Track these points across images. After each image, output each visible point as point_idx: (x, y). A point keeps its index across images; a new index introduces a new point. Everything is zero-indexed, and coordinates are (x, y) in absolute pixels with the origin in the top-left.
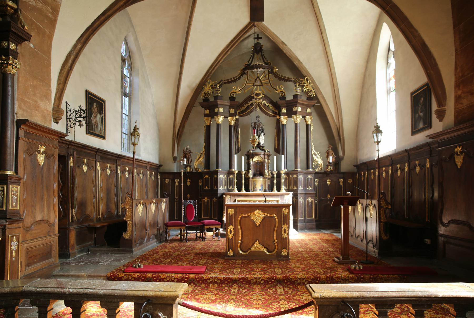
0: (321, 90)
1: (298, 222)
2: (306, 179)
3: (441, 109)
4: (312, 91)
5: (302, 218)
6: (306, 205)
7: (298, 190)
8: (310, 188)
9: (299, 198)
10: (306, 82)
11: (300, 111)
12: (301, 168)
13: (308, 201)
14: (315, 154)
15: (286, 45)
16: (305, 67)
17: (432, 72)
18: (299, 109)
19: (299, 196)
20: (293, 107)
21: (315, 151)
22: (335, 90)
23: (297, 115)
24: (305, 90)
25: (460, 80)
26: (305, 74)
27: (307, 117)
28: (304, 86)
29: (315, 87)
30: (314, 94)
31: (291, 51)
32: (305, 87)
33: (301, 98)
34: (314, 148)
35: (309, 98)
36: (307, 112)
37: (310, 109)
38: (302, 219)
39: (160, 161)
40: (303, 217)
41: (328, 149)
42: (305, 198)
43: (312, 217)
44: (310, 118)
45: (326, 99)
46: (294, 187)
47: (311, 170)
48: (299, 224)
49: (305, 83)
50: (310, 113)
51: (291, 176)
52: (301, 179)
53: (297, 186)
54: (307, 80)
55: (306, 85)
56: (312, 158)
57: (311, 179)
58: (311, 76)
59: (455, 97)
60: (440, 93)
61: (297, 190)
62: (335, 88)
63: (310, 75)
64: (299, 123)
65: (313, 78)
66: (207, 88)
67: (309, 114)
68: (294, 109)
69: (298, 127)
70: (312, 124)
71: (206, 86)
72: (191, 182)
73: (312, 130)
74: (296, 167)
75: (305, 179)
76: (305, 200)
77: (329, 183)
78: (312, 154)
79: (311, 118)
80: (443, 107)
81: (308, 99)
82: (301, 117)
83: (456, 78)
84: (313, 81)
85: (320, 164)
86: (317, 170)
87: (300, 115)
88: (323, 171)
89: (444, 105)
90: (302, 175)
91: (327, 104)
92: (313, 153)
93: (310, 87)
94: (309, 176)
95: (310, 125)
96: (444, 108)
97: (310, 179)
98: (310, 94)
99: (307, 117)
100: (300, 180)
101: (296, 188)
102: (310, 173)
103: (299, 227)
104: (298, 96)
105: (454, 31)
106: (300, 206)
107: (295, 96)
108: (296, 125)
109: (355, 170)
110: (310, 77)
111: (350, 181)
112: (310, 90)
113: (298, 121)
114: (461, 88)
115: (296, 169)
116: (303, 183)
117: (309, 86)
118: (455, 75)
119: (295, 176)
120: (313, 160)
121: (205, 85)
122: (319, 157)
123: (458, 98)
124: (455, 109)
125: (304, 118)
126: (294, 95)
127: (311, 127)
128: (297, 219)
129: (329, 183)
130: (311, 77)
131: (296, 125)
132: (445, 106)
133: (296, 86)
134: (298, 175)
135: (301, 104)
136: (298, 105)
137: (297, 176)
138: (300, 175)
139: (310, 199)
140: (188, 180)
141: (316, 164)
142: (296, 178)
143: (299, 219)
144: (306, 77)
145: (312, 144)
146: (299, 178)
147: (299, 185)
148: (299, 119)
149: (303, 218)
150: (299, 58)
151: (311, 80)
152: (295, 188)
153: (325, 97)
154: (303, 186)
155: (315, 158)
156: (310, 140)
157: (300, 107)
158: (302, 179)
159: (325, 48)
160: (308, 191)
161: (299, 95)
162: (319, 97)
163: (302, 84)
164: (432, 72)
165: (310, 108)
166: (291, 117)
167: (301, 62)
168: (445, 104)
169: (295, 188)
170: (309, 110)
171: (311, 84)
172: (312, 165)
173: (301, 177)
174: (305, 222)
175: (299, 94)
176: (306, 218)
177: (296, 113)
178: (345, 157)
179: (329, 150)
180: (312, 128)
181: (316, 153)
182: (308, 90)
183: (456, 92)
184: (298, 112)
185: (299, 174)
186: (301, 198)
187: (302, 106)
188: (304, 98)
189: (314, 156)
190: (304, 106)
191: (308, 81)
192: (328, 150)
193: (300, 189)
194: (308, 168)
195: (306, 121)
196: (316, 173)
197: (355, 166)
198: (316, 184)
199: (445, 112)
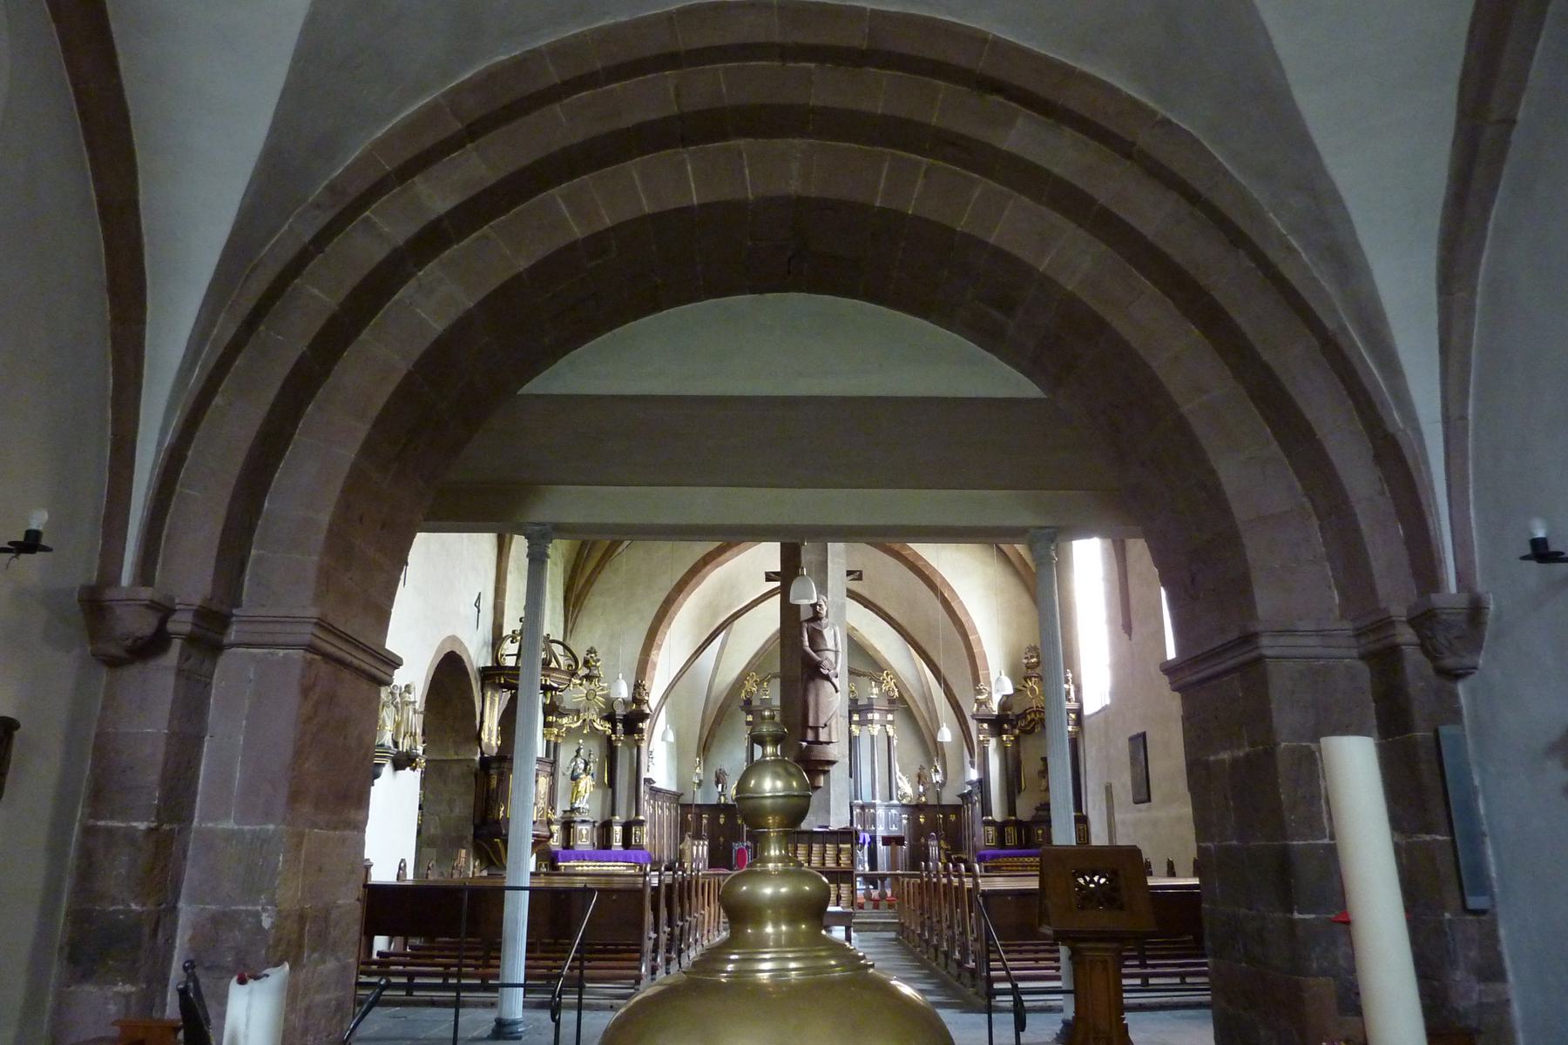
12: (880, 799)
14: (900, 779)
15: (857, 630)
26: (884, 666)
27: (888, 726)
30: (897, 694)
31: (864, 637)
35: (892, 701)
39: (678, 788)
49: (884, 679)
51: (867, 810)
56: (897, 783)
63: (892, 668)
66: (751, 686)
67: (891, 723)
68: (870, 716)
71: (748, 681)
72: (725, 818)
73: (895, 744)
74: (874, 797)
75: (887, 815)
77: (922, 820)
84: (896, 676)
86: (904, 802)
88: (914, 803)
94: (893, 811)
99: (888, 726)
102: (894, 806)
108: (872, 737)
109: (959, 801)
111: (953, 818)
113: (875, 733)
120: (898, 788)
121: (746, 679)
122: (906, 782)
129: (922, 820)
131: (872, 737)
140: (722, 816)
146: (877, 813)
147: (878, 824)
150: (876, 646)
151: (894, 675)
152: (873, 828)
155: (900, 784)
162: (906, 696)
167: (878, 651)
170: (890, 717)
172: (897, 794)
173: (881, 812)
177: (871, 722)
180: (895, 742)
181: (902, 777)
189: (898, 780)
194: (891, 798)
195: (887, 732)
196: (903, 805)
197: (959, 796)
198: (905, 822)
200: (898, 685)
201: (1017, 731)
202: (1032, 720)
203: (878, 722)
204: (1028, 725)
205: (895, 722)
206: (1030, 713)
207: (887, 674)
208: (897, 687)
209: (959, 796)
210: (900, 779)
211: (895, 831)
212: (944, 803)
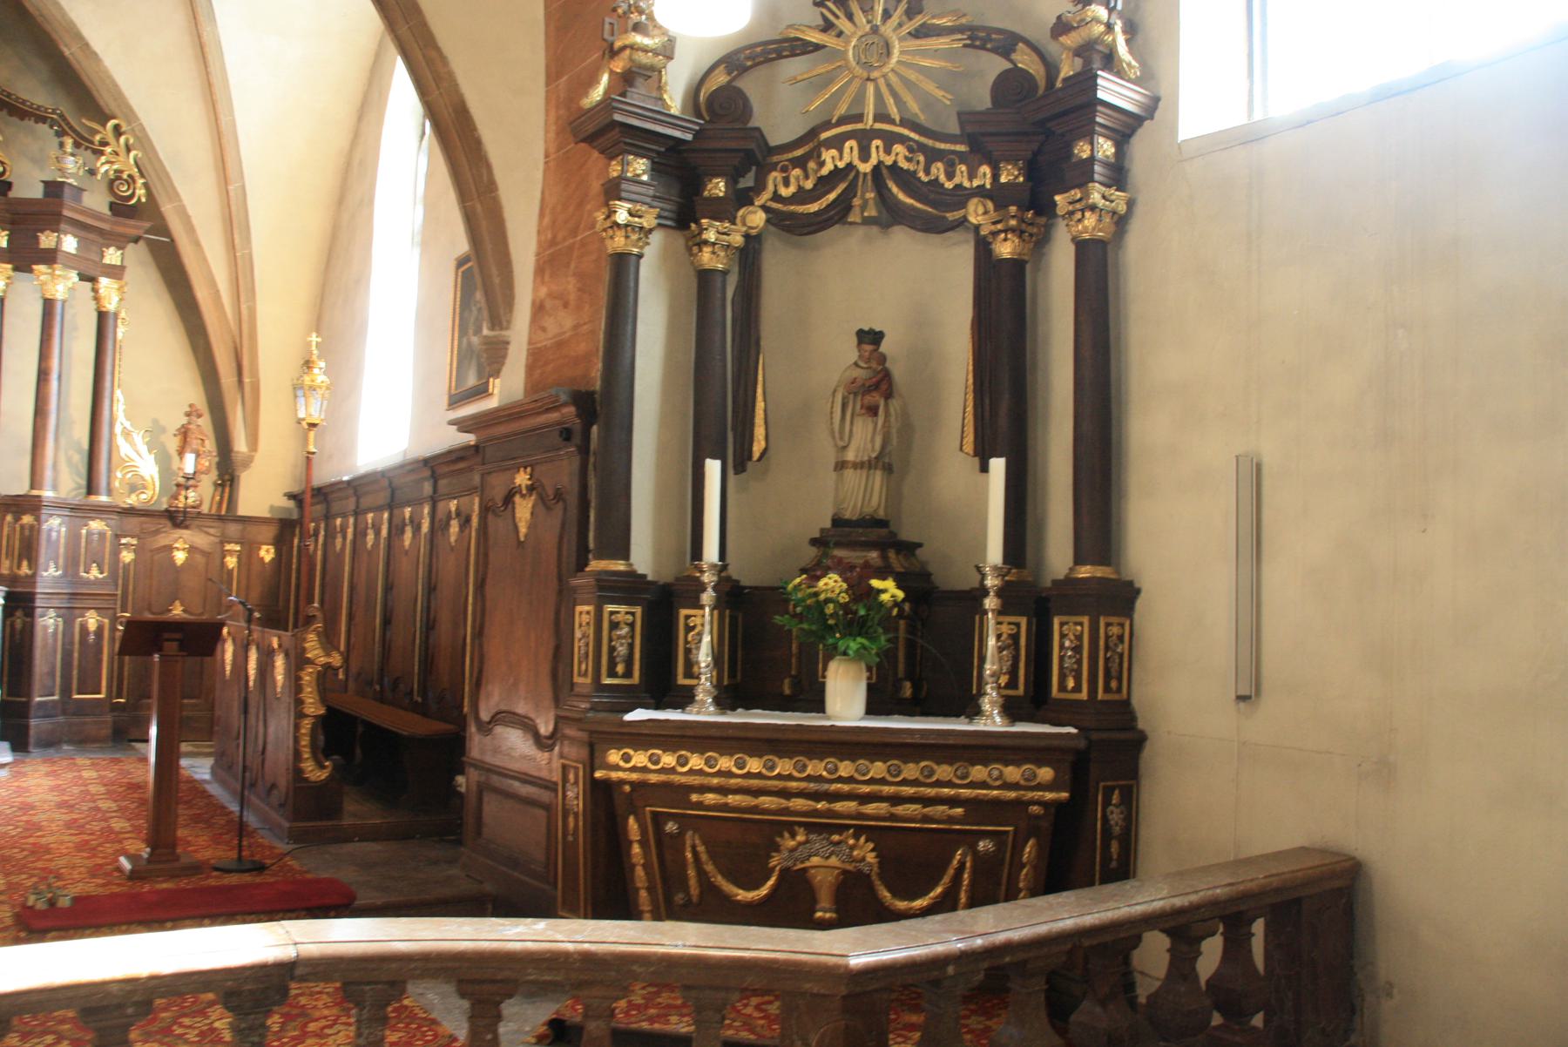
0: (176, 184)
1: (32, 712)
2: (79, 536)
3: (495, 337)
4: (134, 182)
5: (53, 695)
6: (72, 643)
7: (38, 579)
8: (95, 573)
9: (38, 611)
10: (110, 137)
11: (74, 252)
13: (84, 629)
14: (127, 434)
16: (110, 77)
17: (479, 207)
18: (70, 244)
19: (38, 603)
20: (42, 231)
21: (128, 424)
22: (232, 194)
23: (56, 266)
24: (103, 170)
25: (547, 253)
28: (102, 153)
29: (149, 166)
30: (141, 192)
32: (103, 159)
33: (78, 199)
34: (124, 411)
35: (121, 208)
36: (107, 261)
37: (119, 252)
38: (53, 701)
40: (57, 690)
41: (184, 420)
42: (69, 614)
43: (99, 693)
44: (116, 286)
45: (195, 221)
46: (19, 567)
47: (103, 499)
48: (33, 722)
49: (104, 143)
50: (114, 266)
52: (54, 534)
53: (33, 562)
54: (118, 131)
55: (108, 150)
57: (102, 535)
58: (137, 119)
59: (534, 303)
60: (497, 280)
61: (34, 576)
62: (231, 188)
63: (131, 116)
64: (64, 302)
65: (143, 129)
67: (116, 272)
68: (47, 240)
69: (58, 318)
70: (123, 314)
75: (74, 538)
76: (69, 623)
78: (112, 433)
79: (120, 289)
80: (501, 329)
81: (112, 206)
82: (76, 279)
83: (539, 243)
84: (144, 141)
85: (148, 478)
86: (132, 500)
87: (68, 267)
89: (505, 324)
90: (59, 515)
91: (197, 244)
92: (118, 429)
93: (127, 164)
94: (96, 525)
95: (116, 315)
96: (504, 333)
97: (96, 537)
98: (123, 190)
99: (104, 282)
100: (49, 536)
101: (30, 568)
103: (32, 732)
104: (67, 191)
105: (547, 92)
106: (45, 646)
107: (54, 189)
110: (129, 123)
112: (125, 176)
113: (59, 291)
114: (547, 278)
115: (35, 492)
116: (62, 550)
117: (121, 159)
118: (539, 232)
119: (27, 519)
122: (143, 449)
123: (539, 309)
124: (530, 342)
125: (88, 285)
126: (46, 184)
127: (116, 326)
128: (24, 699)
130: (134, 125)
131: (48, 306)
132: (507, 328)
133: (62, 145)
134: (43, 517)
135: (80, 227)
136: (63, 226)
137: (38, 519)
138: (51, 515)
139: (92, 621)
141: (129, 475)
142: (32, 527)
143: (38, 699)
144: (114, 117)
145: (118, 393)
146: (45, 527)
147: (42, 559)
148: (62, 284)
149: (56, 698)
151: (136, 137)
153: (191, 211)
154: (61, 561)
155: (123, 448)
156: (108, 378)
157: (75, 236)
158: (59, 532)
159: (196, 24)
160: (88, 583)
161: (70, 184)
162: (167, 208)
163: (92, 143)
164: (479, 207)
165: (119, 248)
166: (31, 271)
168: (509, 322)
169: (25, 570)
171: (132, 154)
173: (54, 526)
174: (64, 713)
175: (70, 181)
176: (70, 697)
177: (50, 257)
178: (258, 457)
179: (189, 423)
182: (116, 171)
183: (535, 290)
184: (60, 257)
185: (44, 511)
186: (52, 613)
187: (83, 234)
188: (96, 201)
189: (120, 440)
190: (92, 236)
191: (122, 139)
192: (183, 426)
193: (45, 574)
195: (97, 299)
199: (507, 349)
200: (148, 168)
201: (757, 219)
202: (837, 174)
203: (71, 261)
204: (802, 196)
205: (128, 275)
206: (837, 143)
207: (118, 131)
208: (142, 175)
209: (291, 496)
210: (127, 434)
211: (97, 582)
212: (243, 509)
